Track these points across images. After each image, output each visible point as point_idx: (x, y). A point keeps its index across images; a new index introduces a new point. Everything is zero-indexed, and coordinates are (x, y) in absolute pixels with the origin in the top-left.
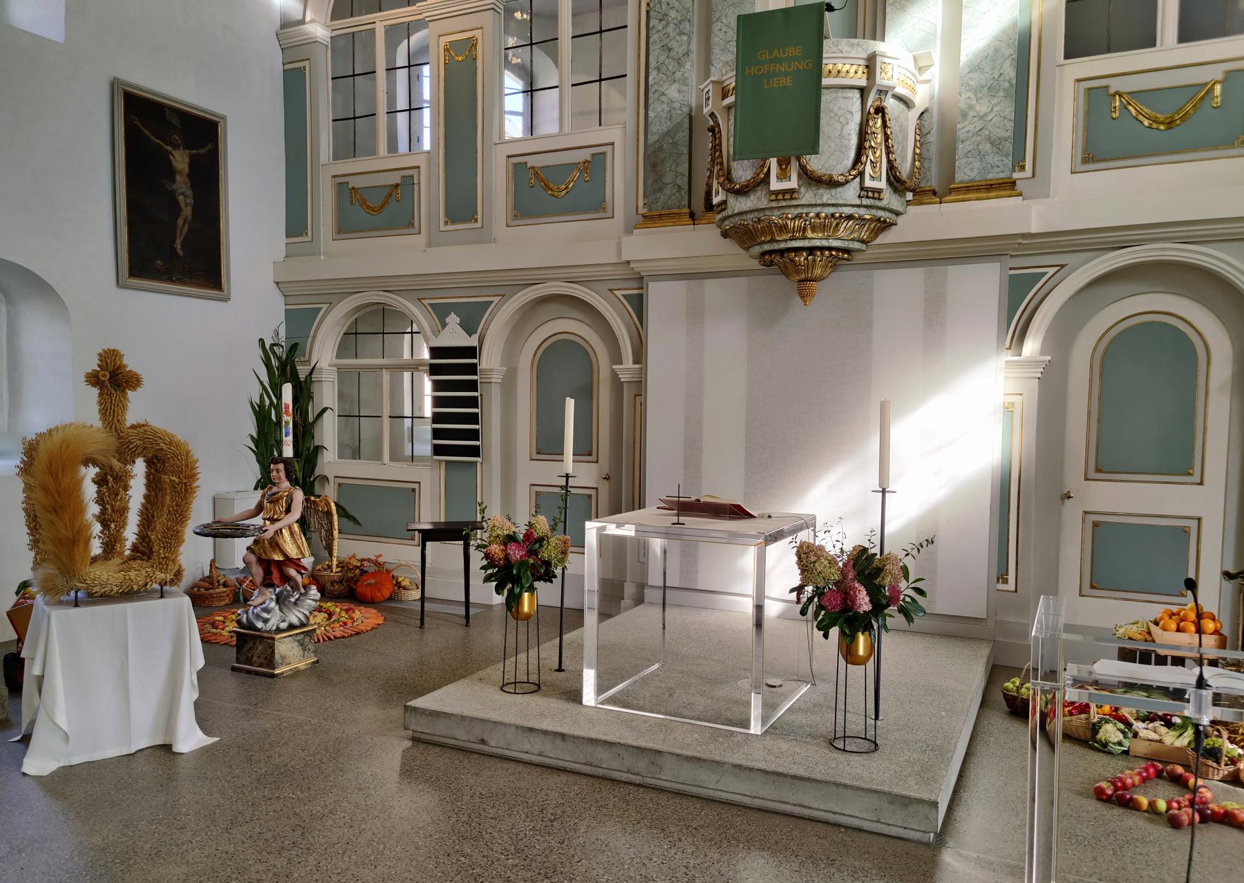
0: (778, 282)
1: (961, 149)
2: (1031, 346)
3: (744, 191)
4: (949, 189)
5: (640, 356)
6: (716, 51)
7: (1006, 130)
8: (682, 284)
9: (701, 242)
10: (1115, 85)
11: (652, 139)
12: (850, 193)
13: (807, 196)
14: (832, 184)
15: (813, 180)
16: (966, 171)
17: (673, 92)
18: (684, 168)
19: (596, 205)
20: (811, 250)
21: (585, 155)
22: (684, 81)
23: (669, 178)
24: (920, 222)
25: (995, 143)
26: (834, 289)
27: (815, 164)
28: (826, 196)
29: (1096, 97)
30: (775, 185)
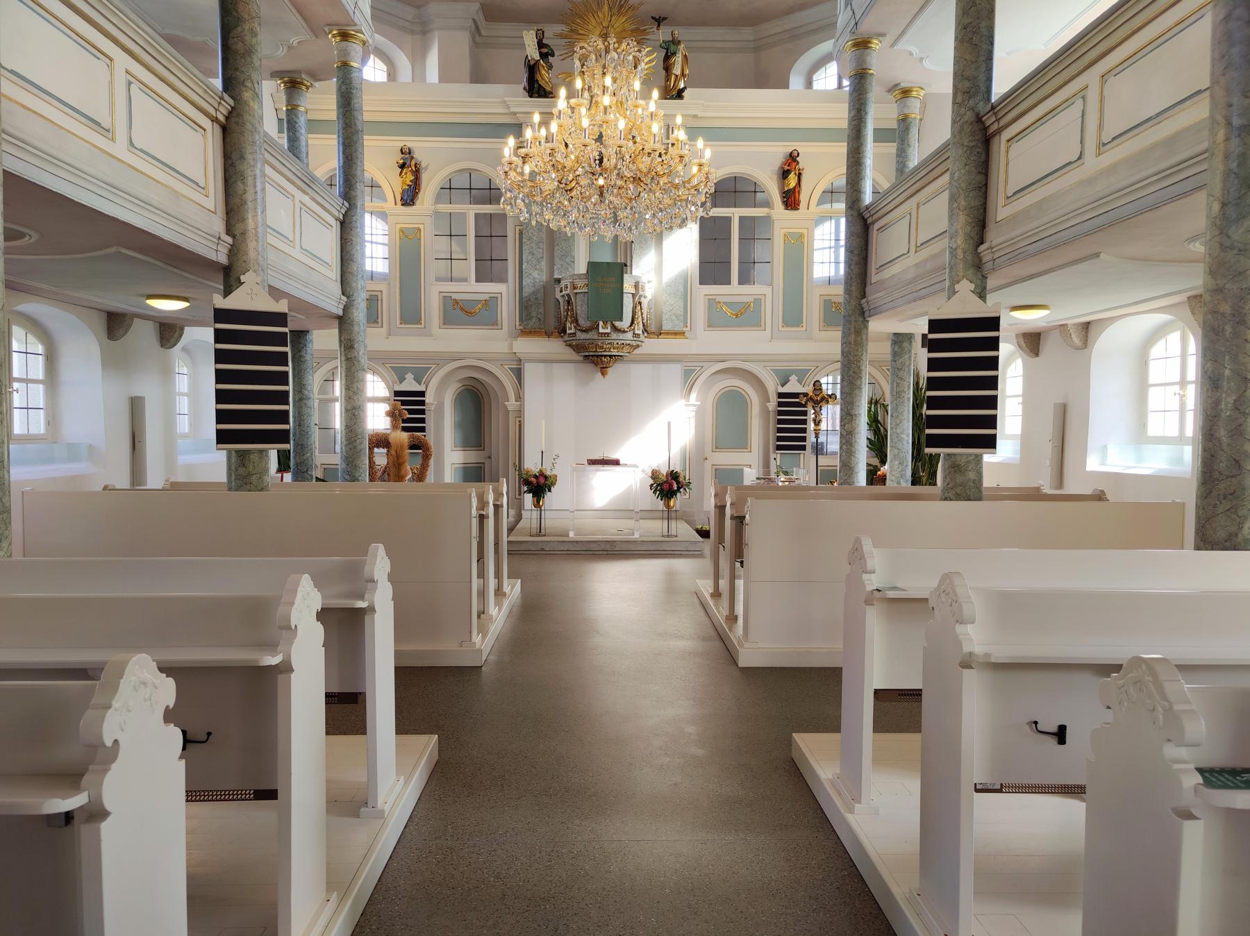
0: (589, 367)
1: (665, 317)
2: (693, 396)
3: (586, 331)
4: (659, 334)
5: (519, 398)
6: (556, 259)
7: (680, 311)
8: (542, 365)
9: (554, 346)
10: (718, 299)
11: (525, 295)
12: (629, 335)
13: (614, 336)
14: (624, 332)
15: (615, 329)
16: (666, 327)
17: (535, 274)
18: (541, 310)
19: (493, 323)
20: (611, 356)
21: (486, 297)
22: (541, 270)
23: (534, 314)
24: (651, 346)
25: (677, 316)
26: (615, 370)
27: (617, 324)
28: (621, 336)
29: (712, 303)
30: (601, 330)
